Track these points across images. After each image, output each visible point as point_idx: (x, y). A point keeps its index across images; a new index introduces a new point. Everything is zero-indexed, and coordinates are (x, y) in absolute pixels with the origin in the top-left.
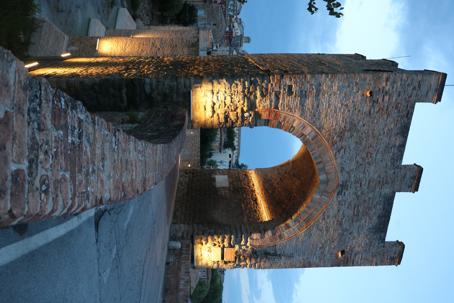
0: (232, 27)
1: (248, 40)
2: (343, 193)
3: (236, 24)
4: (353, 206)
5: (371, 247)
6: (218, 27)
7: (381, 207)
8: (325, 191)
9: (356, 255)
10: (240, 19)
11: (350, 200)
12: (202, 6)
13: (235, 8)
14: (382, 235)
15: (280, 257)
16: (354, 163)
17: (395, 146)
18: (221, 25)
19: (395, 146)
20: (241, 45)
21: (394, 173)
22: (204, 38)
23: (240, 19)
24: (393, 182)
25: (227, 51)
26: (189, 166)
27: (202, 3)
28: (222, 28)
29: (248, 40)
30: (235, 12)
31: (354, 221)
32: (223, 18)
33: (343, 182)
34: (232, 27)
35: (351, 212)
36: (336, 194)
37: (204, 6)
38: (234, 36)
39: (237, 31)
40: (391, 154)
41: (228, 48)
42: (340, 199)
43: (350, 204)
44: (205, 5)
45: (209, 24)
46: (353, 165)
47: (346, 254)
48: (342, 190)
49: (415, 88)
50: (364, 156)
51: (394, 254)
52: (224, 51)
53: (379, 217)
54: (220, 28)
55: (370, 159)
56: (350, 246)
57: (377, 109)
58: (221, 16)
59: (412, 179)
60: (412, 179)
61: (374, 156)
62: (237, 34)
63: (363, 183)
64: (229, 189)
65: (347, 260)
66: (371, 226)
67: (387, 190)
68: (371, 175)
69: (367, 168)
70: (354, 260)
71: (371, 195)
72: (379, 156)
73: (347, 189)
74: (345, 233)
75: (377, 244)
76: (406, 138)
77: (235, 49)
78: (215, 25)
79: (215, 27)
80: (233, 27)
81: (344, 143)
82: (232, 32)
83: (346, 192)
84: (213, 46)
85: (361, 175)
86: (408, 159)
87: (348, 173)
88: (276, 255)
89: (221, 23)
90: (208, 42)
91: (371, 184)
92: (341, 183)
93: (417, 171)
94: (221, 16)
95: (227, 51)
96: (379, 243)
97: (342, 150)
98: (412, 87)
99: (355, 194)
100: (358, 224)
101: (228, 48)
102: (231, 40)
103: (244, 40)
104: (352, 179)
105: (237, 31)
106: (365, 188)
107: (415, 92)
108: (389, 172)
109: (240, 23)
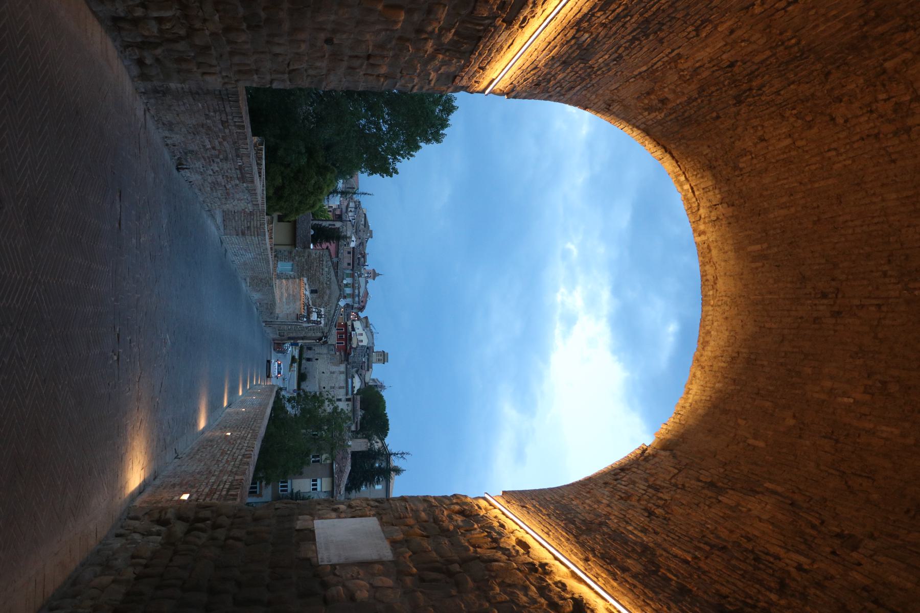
0: (350, 328)
1: (384, 357)
3: (357, 324)
10: (366, 318)
12: (286, 253)
13: (357, 291)
18: (328, 292)
20: (369, 367)
22: (289, 295)
23: (366, 318)
25: (341, 373)
26: (185, 497)
27: (288, 248)
28: (329, 297)
29: (384, 357)
30: (357, 299)
32: (333, 278)
34: (350, 328)
37: (290, 253)
38: (354, 346)
39: (360, 337)
41: (342, 368)
44: (295, 251)
52: (334, 373)
54: (326, 298)
58: (329, 273)
62: (361, 344)
64: (396, 569)
77: (357, 372)
79: (315, 295)
80: (353, 329)
82: (351, 339)
84: (309, 313)
89: (330, 288)
90: (298, 304)
94: (329, 273)
95: (341, 373)
101: (342, 368)
102: (349, 354)
103: (374, 357)
105: (360, 338)
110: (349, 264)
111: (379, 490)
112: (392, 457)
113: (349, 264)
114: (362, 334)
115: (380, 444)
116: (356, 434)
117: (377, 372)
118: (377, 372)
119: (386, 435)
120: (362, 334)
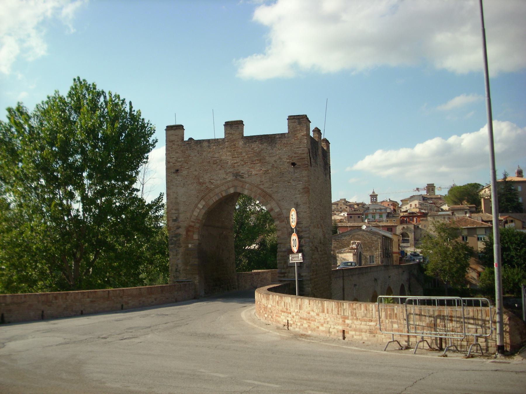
0: (405, 214)
1: (431, 188)
3: (404, 208)
8: (242, 187)
9: (295, 153)
10: (401, 201)
14: (278, 137)
16: (220, 172)
17: (209, 146)
19: (209, 146)
23: (401, 201)
29: (431, 188)
33: (233, 176)
34: (405, 214)
36: (243, 179)
38: (418, 210)
39: (413, 207)
40: (214, 147)
42: (247, 176)
43: (251, 168)
46: (222, 171)
49: (174, 144)
50: (215, 165)
51: (299, 121)
56: (287, 159)
59: (234, 126)
60: (234, 126)
62: (417, 206)
63: (235, 162)
66: (269, 148)
67: (241, 143)
74: (275, 166)
76: (203, 140)
80: (406, 211)
81: (207, 181)
82: (413, 213)
86: (220, 134)
87: (227, 174)
92: (234, 177)
93: (229, 125)
97: (212, 181)
98: (173, 146)
99: (243, 165)
100: (267, 158)
101: (429, 218)
104: (231, 170)
105: (413, 206)
106: (238, 160)
107: (176, 143)
110: (359, 217)
111: (522, 189)
114: (411, 205)
117: (442, 191)
118: (442, 191)
120: (411, 205)
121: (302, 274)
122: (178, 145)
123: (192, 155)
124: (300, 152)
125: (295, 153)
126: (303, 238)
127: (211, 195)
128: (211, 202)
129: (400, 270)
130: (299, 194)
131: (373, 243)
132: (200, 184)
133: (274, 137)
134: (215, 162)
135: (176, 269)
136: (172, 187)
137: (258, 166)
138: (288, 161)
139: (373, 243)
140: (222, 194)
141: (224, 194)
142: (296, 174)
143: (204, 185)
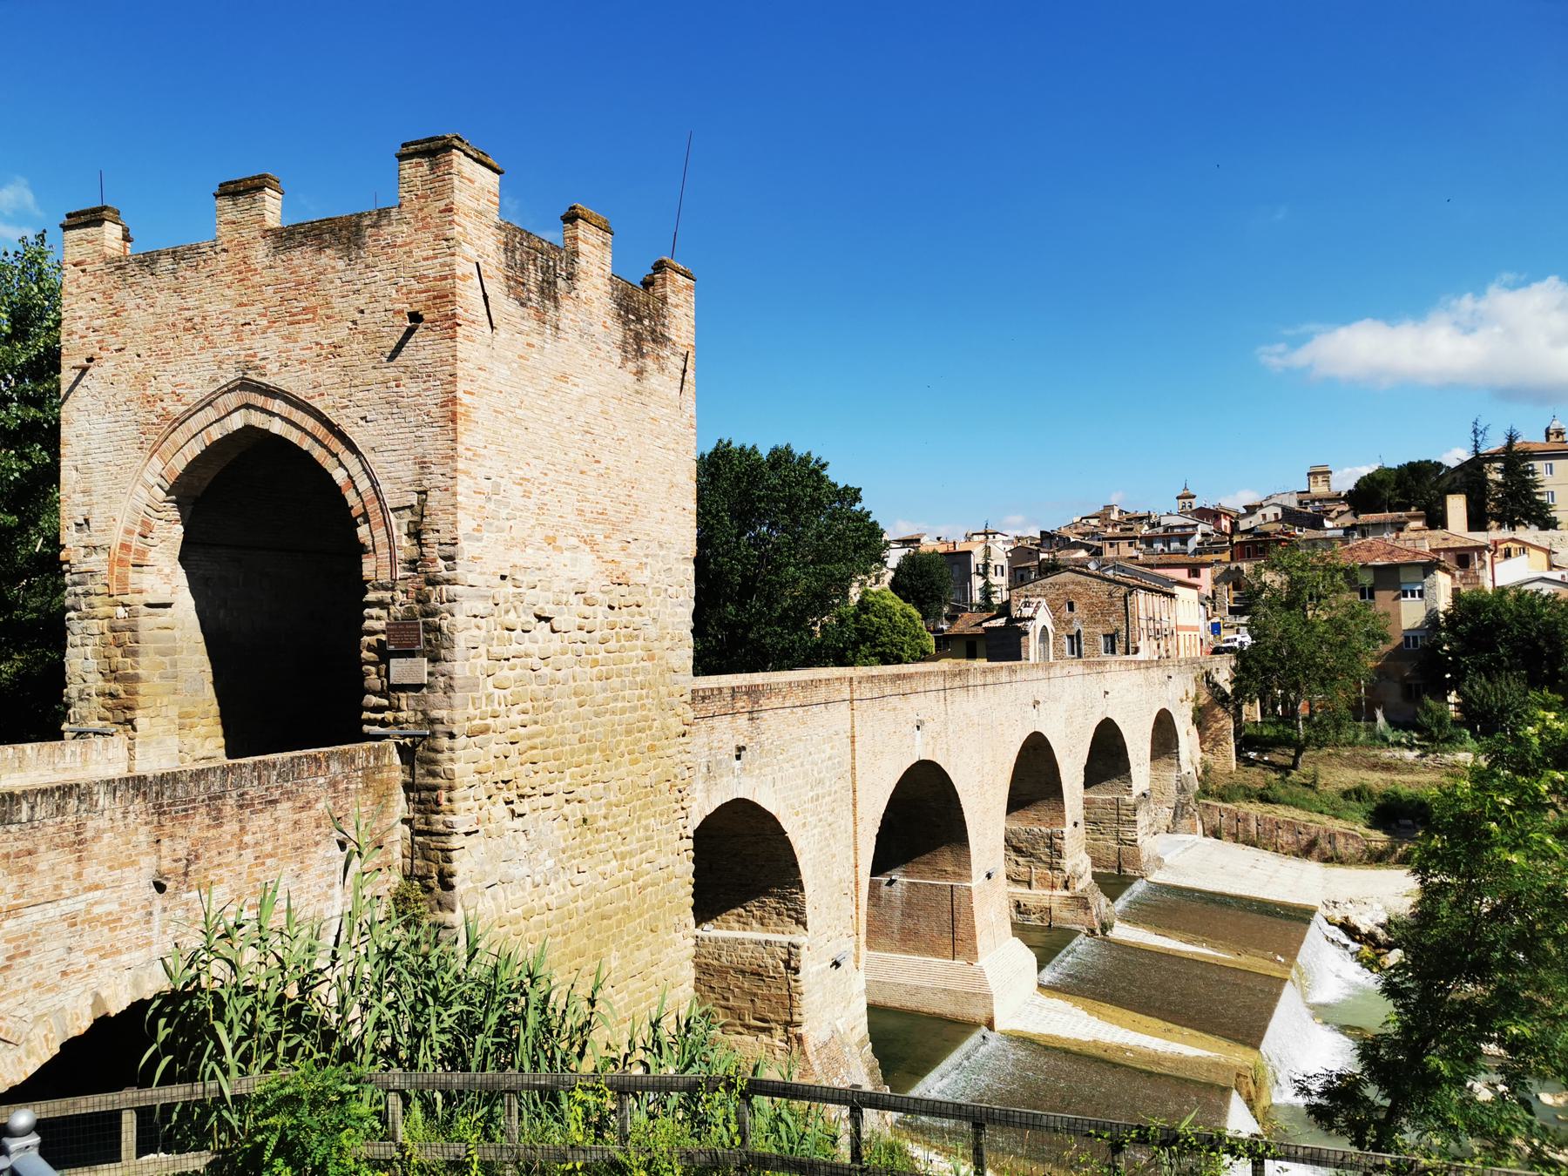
2: (263, 363)
3: (1244, 525)
4: (291, 329)
5: (399, 241)
6: (1078, 595)
7: (296, 253)
11: (279, 340)
14: (367, 222)
15: (425, 492)
19: (174, 272)
21: (224, 250)
24: (242, 246)
28: (1079, 584)
31: (329, 312)
35: (306, 327)
45: (1070, 622)
46: (207, 356)
47: (416, 308)
48: (256, 368)
53: (320, 250)
54: (1079, 589)
55: (196, 320)
57: (110, 339)
58: (1043, 587)
61: (187, 314)
65: (435, 298)
66: (341, 265)
68: (227, 306)
69: (214, 322)
70: (435, 279)
71: (270, 290)
72: (191, 302)
73: (255, 356)
74: (360, 328)
75: (391, 229)
78: (1071, 608)
79: (1076, 606)
83: (260, 355)
85: (228, 329)
88: (422, 503)
91: (245, 300)
96: (390, 224)
107: (89, 268)
108: (222, 266)
109: (1251, 510)
110: (1130, 545)
112: (1482, 450)
113: (1130, 545)
114: (1264, 516)
115: (1459, 475)
116: (1436, 520)
118: (1345, 480)
119: (1439, 465)
120: (1264, 516)
121: (435, 714)
122: (94, 274)
123: (130, 305)
124: (431, 273)
125: (419, 279)
126: (439, 583)
127: (179, 436)
128: (179, 464)
129: (1157, 674)
130: (431, 424)
131: (1112, 604)
132: (149, 401)
133: (358, 225)
134: (189, 325)
135: (81, 691)
136: (75, 415)
137: (307, 333)
138: (398, 306)
139: (1112, 604)
140: (209, 435)
141: (216, 433)
142: (422, 354)
143: (158, 407)
